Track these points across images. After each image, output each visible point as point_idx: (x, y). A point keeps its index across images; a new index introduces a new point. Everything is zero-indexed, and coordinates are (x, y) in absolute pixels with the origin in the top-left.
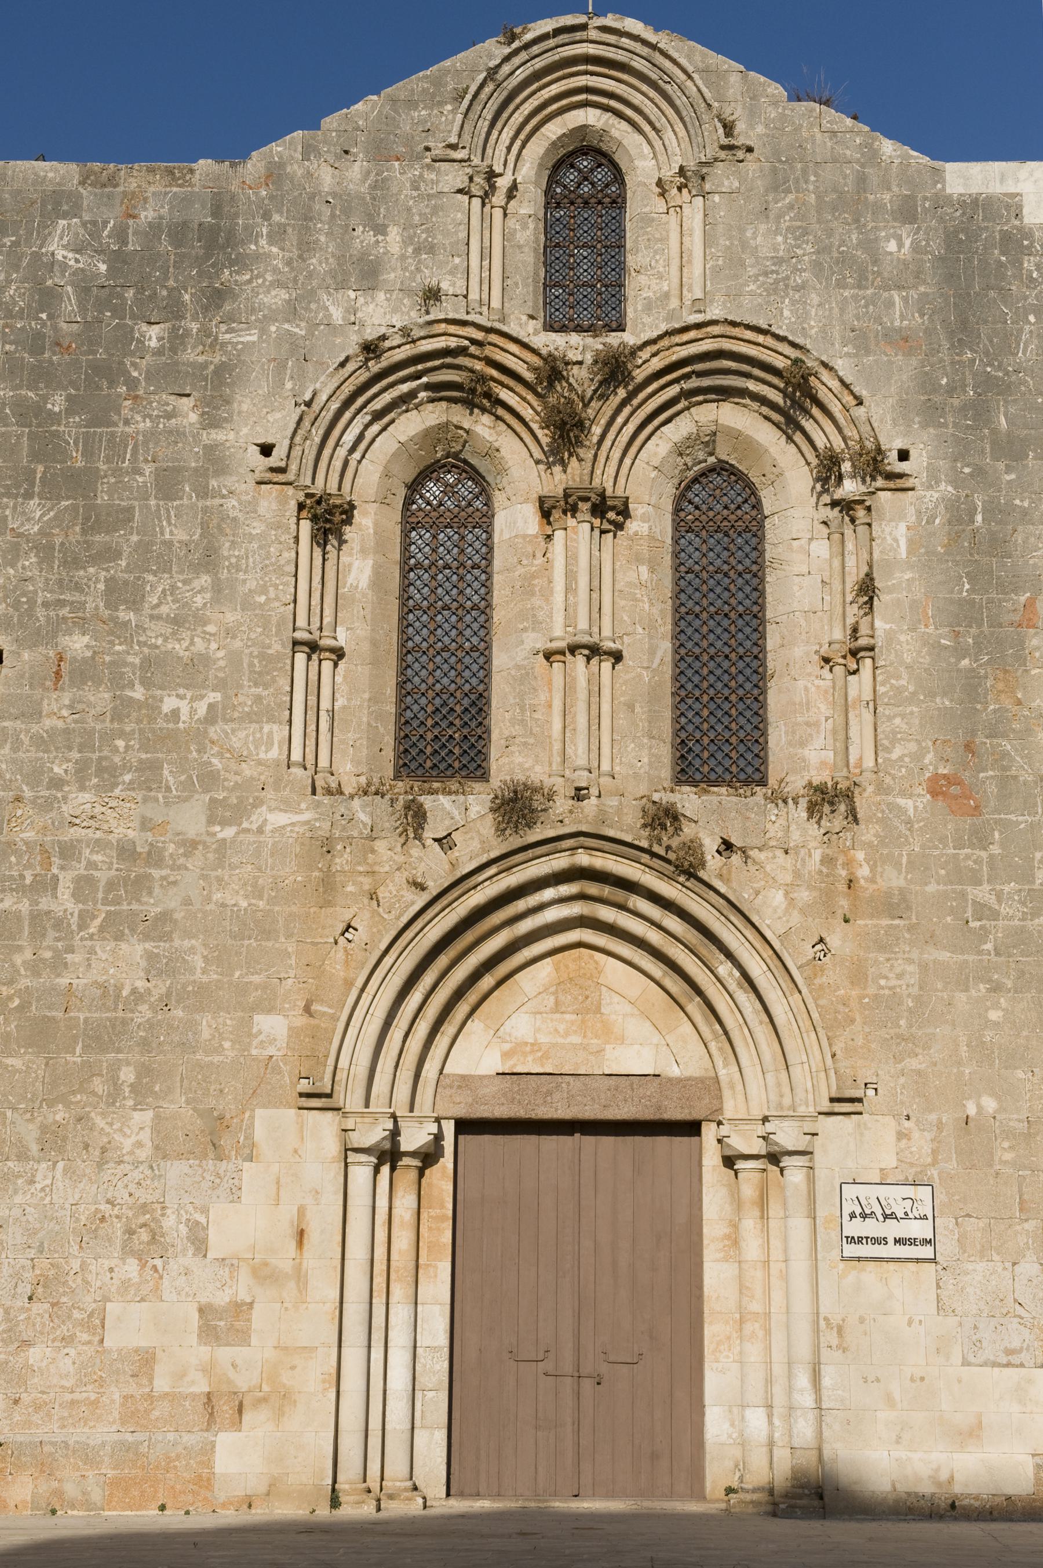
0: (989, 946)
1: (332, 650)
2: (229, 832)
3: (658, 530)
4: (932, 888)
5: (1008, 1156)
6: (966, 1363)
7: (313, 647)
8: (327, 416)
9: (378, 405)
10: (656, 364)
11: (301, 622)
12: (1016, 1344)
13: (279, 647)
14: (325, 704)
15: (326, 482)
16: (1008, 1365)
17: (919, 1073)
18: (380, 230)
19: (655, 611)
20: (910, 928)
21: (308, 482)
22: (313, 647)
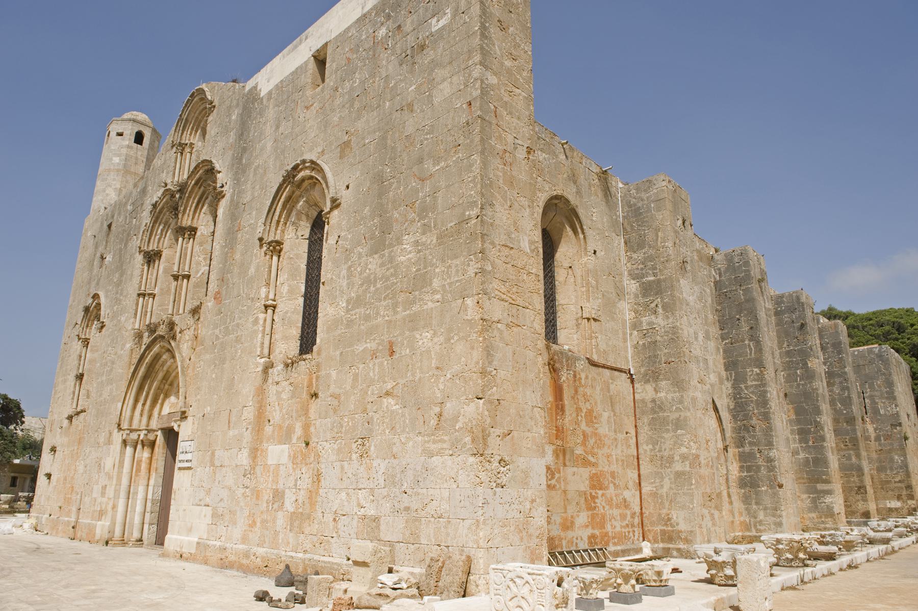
0: (216, 351)
1: (151, 294)
2: (122, 352)
3: (206, 233)
4: (209, 333)
5: (209, 428)
6: (193, 505)
7: (144, 295)
8: (150, 228)
9: (163, 221)
10: (193, 182)
11: (143, 288)
12: (201, 498)
13: (135, 296)
14: (149, 310)
15: (153, 246)
16: (199, 505)
17: (199, 400)
18: (163, 172)
19: (201, 259)
20: (204, 348)
21: (146, 248)
22: (144, 295)
